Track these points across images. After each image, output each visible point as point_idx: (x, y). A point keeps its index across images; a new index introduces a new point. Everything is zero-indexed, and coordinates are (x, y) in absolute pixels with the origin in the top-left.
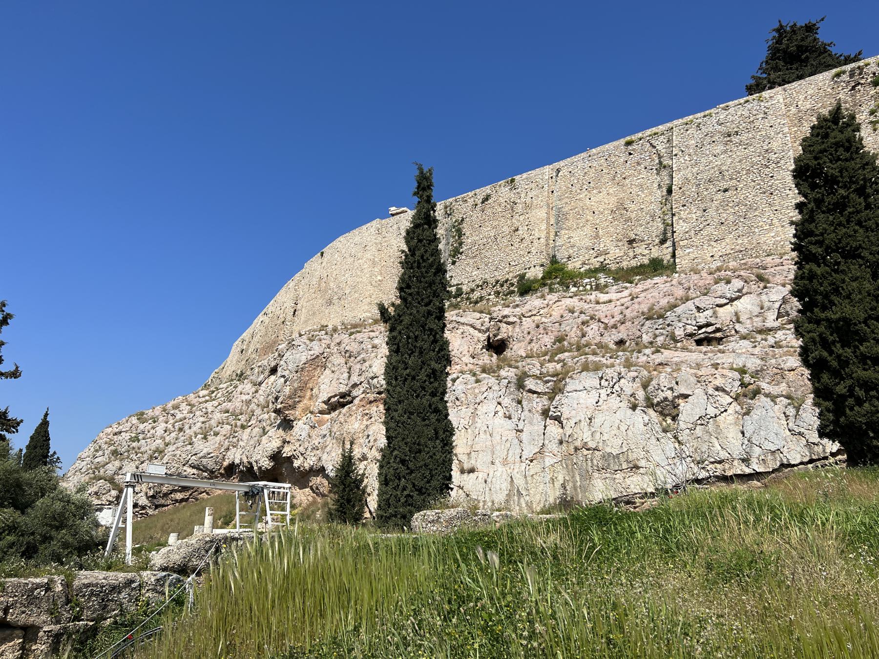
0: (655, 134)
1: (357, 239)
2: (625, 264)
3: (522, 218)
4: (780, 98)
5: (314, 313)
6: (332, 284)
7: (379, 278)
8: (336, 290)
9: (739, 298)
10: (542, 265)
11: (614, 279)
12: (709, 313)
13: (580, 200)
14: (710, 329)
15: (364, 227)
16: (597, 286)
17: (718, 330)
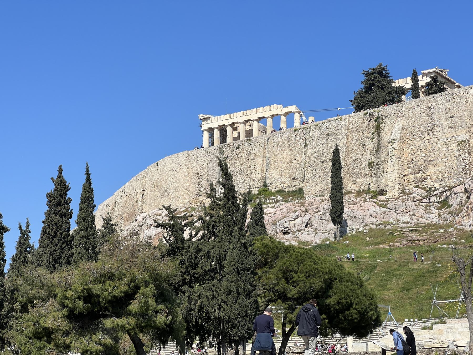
0: (305, 128)
1: (176, 160)
2: (290, 189)
3: (252, 161)
4: (347, 120)
5: (155, 200)
6: (164, 185)
7: (188, 184)
8: (166, 189)
9: (297, 218)
10: (258, 188)
11: (282, 198)
12: (288, 223)
13: (276, 155)
14: (287, 229)
15: (180, 154)
16: (276, 200)
17: (289, 229)
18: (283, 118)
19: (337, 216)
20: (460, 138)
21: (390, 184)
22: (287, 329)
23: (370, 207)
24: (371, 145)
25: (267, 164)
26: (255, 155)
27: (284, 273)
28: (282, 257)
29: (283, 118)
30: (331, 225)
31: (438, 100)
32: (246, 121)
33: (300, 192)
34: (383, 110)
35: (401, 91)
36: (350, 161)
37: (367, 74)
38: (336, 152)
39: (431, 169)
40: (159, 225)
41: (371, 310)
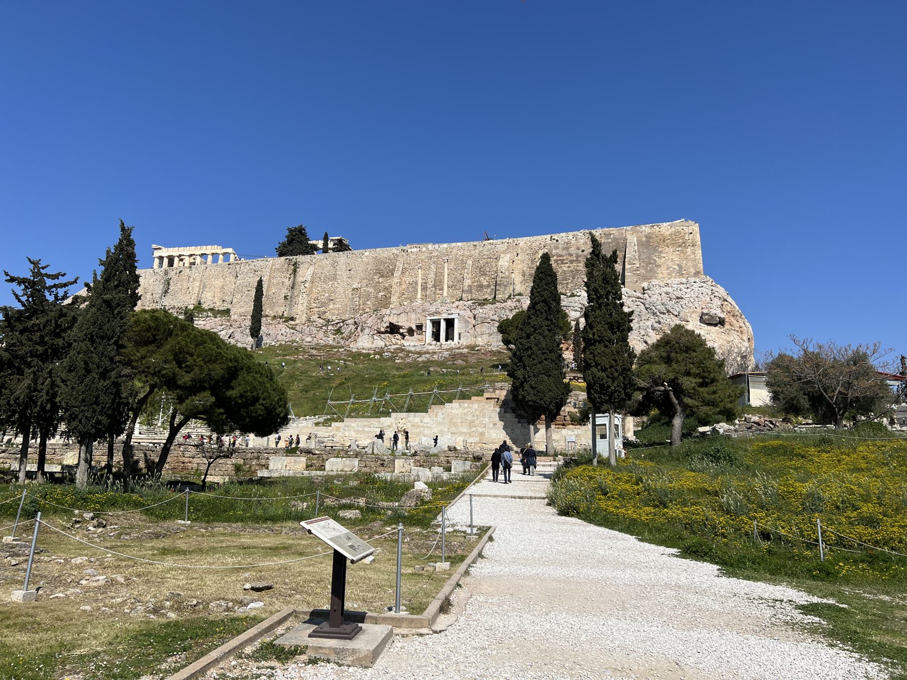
18: (221, 256)
19: (255, 331)
20: (354, 286)
21: (300, 313)
22: (177, 421)
23: (283, 328)
24: (288, 283)
25: (204, 287)
26: (194, 279)
27: (176, 355)
28: (177, 335)
29: (221, 256)
30: (250, 339)
31: (342, 256)
32: (191, 255)
33: (227, 312)
34: (300, 258)
35: (314, 248)
36: (270, 293)
37: (290, 231)
38: (260, 283)
39: (331, 306)
40: (12, 280)
41: (280, 406)
